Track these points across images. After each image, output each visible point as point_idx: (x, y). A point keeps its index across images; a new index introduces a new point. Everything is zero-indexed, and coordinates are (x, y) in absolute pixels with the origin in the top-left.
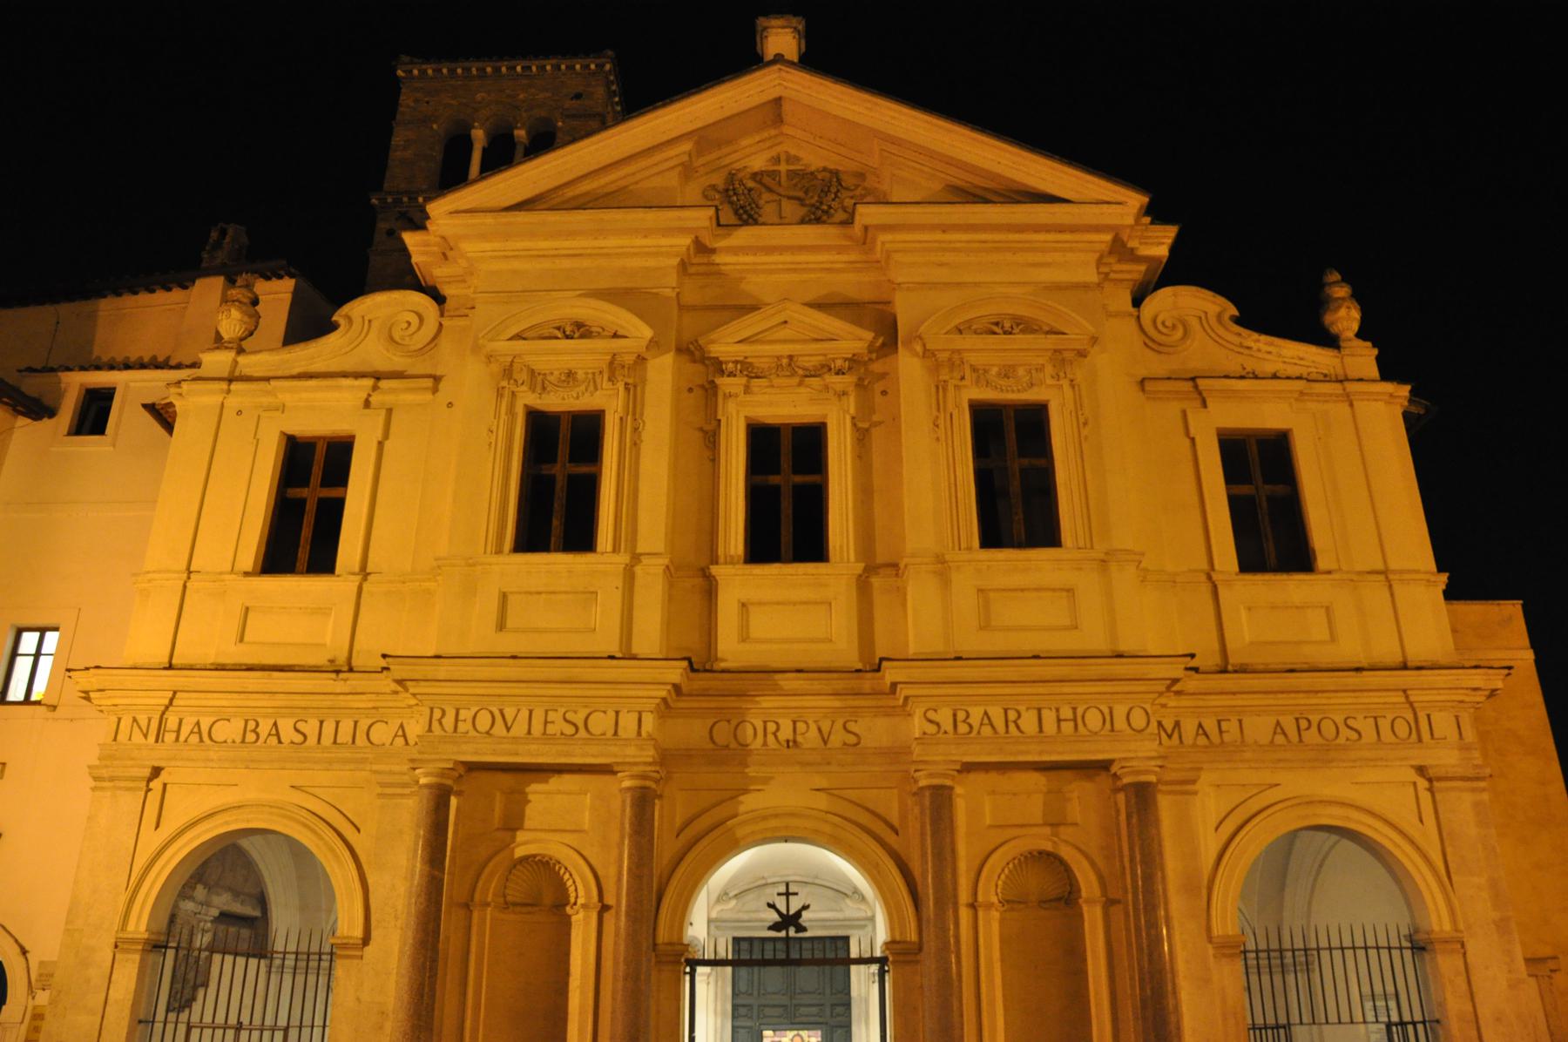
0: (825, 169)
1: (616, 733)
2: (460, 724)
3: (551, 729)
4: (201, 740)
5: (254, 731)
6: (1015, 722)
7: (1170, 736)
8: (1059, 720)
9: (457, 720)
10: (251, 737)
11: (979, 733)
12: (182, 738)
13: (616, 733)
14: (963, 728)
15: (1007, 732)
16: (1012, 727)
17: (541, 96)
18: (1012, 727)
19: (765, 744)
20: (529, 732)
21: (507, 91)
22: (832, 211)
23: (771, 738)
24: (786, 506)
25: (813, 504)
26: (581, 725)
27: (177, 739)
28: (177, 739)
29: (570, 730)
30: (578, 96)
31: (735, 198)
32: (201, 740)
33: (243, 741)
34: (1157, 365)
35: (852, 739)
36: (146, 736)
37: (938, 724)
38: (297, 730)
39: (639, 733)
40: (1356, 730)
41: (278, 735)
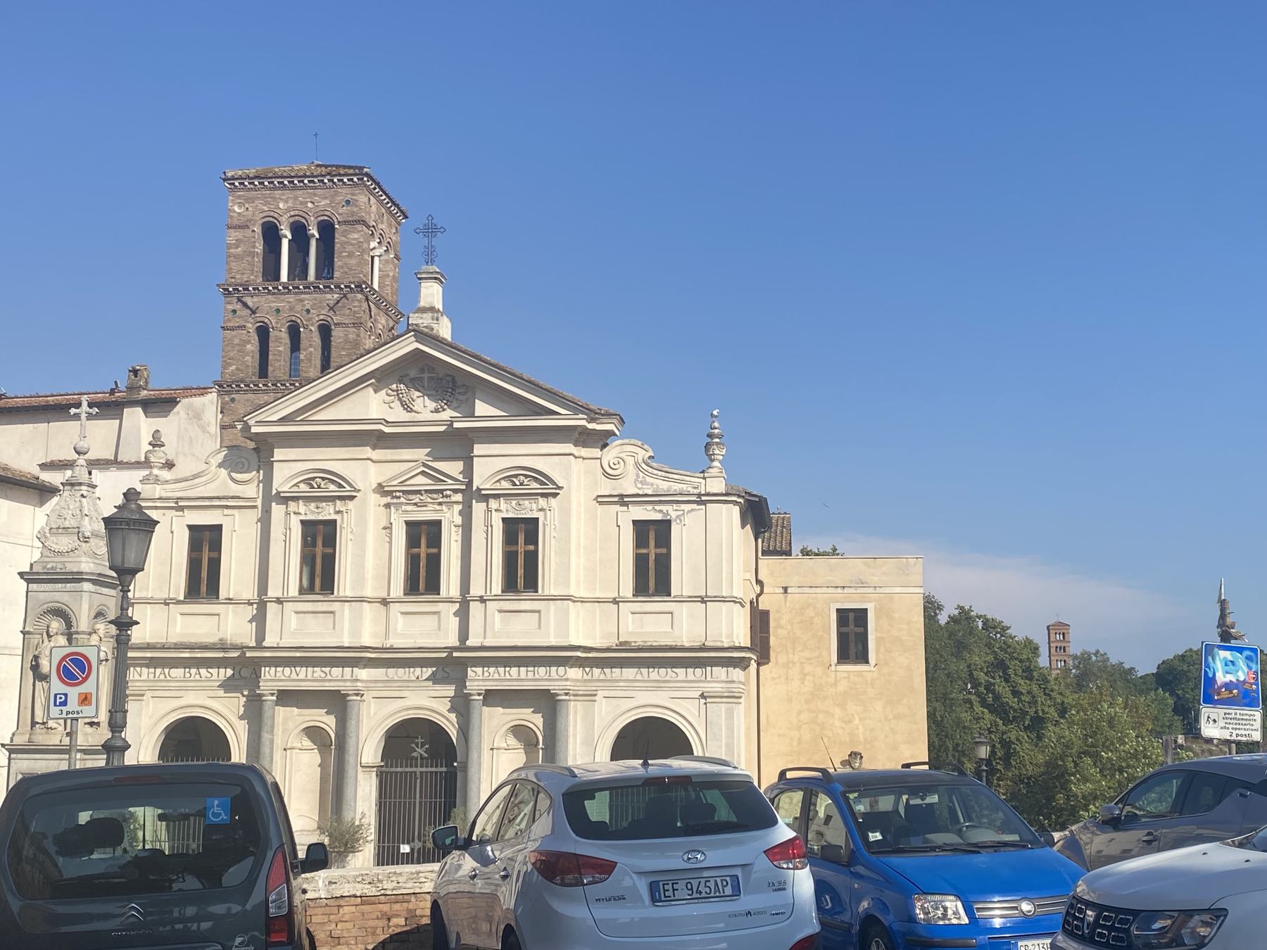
0: (448, 375)
1: (342, 676)
2: (277, 673)
3: (315, 675)
4: (165, 677)
5: (189, 672)
6: (509, 672)
7: (587, 674)
8: (527, 671)
9: (276, 671)
10: (188, 675)
11: (493, 676)
12: (157, 676)
13: (342, 676)
14: (486, 674)
15: (505, 676)
16: (507, 674)
17: (323, 203)
18: (507, 674)
19: (409, 677)
20: (306, 676)
21: (300, 199)
22: (449, 403)
23: (411, 674)
24: (423, 563)
25: (434, 563)
26: (328, 673)
27: (155, 677)
28: (155, 677)
29: (323, 675)
30: (348, 202)
31: (401, 396)
32: (165, 677)
33: (184, 677)
34: (606, 488)
35: (446, 675)
36: (140, 676)
37: (476, 672)
38: (208, 672)
39: (352, 677)
40: (676, 673)
41: (200, 674)
